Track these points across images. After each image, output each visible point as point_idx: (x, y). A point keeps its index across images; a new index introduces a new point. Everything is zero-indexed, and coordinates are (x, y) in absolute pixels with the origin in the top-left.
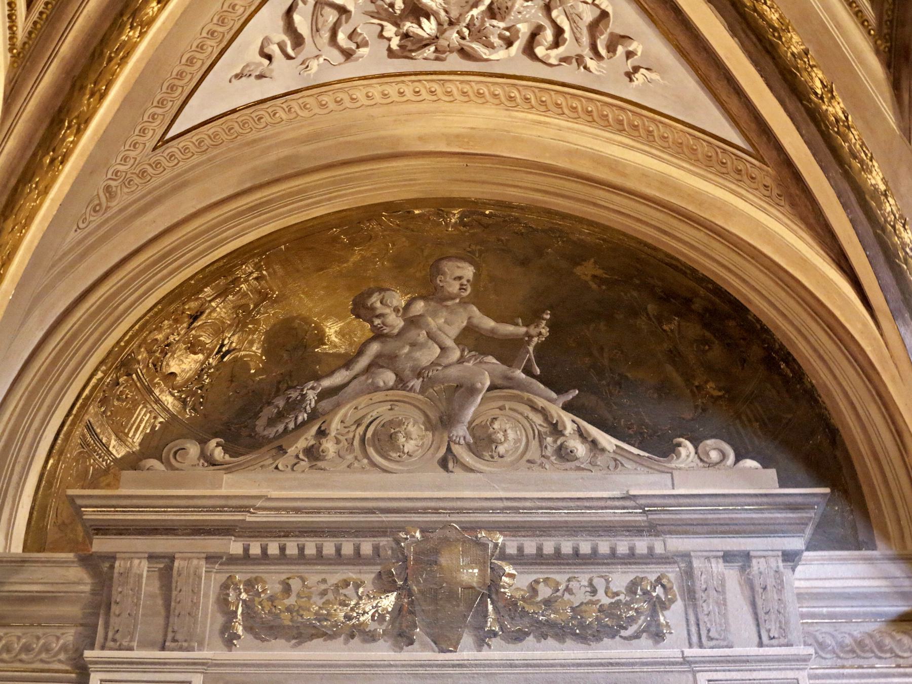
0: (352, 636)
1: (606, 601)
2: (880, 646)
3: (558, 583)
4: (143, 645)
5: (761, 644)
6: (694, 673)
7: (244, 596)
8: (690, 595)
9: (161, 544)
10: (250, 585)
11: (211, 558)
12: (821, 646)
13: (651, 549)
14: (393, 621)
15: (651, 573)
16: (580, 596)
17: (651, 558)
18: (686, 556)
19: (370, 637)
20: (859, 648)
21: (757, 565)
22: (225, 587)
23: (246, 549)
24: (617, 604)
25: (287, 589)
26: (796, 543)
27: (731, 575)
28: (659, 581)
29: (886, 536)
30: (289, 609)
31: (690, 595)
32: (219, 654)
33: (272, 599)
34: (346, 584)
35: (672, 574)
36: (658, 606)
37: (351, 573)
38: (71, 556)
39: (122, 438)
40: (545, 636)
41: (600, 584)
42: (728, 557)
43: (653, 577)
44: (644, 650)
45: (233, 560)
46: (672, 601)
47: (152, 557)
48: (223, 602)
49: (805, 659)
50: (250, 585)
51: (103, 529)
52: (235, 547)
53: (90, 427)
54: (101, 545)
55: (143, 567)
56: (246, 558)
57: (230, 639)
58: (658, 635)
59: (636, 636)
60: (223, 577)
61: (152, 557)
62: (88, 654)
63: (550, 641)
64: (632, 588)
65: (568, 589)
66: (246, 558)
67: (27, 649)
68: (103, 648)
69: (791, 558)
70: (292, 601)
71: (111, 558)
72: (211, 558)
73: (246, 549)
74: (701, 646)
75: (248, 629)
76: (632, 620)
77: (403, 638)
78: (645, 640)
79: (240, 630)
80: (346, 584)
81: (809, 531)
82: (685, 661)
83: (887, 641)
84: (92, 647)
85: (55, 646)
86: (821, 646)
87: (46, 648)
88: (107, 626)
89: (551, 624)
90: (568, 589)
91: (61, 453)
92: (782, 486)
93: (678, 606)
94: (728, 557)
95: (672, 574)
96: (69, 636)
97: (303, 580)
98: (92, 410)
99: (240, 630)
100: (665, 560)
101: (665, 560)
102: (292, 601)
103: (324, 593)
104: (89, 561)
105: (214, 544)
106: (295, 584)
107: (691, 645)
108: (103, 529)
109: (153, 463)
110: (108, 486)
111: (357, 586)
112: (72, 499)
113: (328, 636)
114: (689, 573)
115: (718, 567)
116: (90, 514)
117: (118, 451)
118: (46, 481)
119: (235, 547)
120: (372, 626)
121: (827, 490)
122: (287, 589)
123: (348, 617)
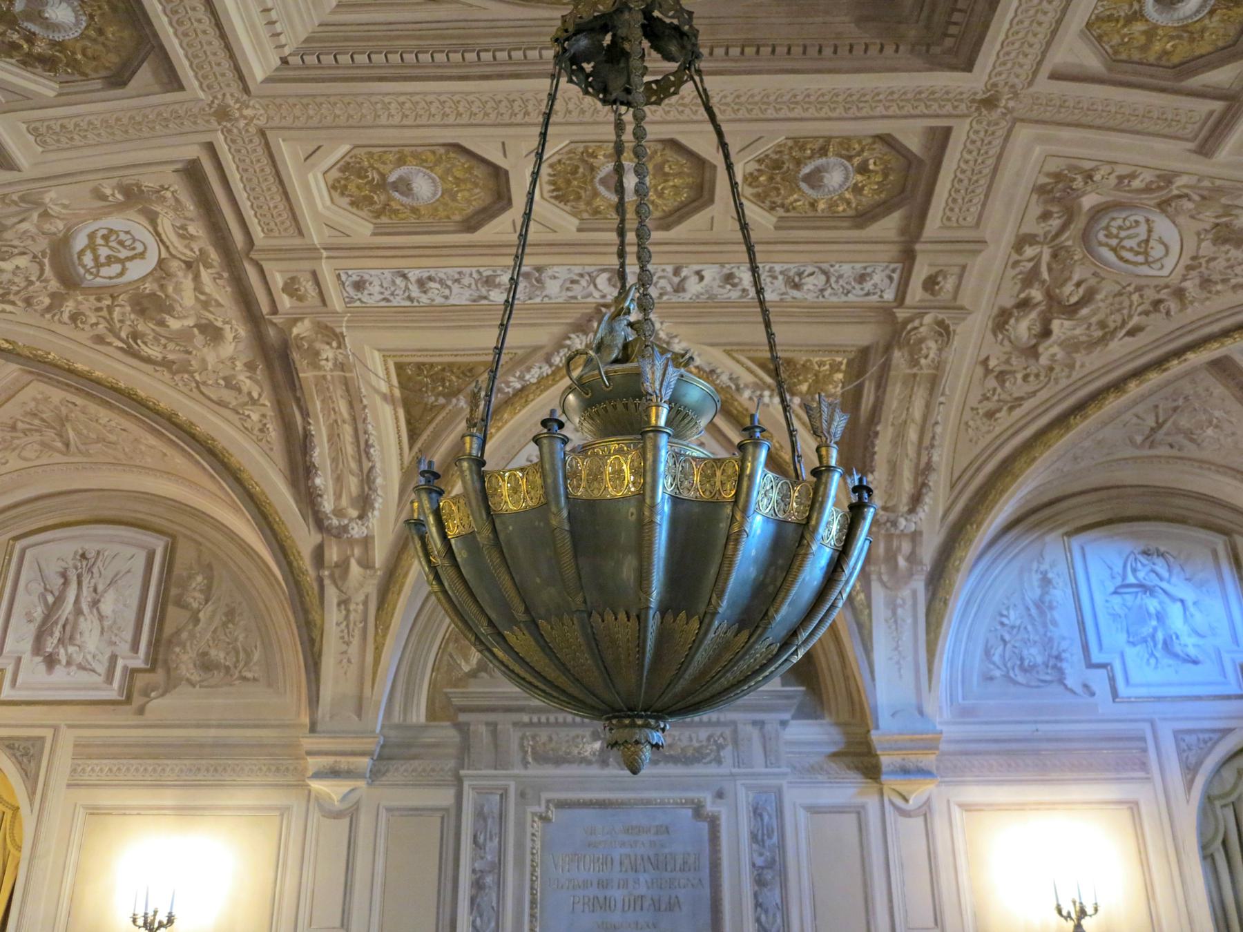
0: (581, 762)
1: (696, 745)
2: (821, 768)
3: (674, 736)
4: (487, 767)
5: (766, 767)
6: (735, 780)
7: (531, 743)
8: (735, 742)
9: (491, 717)
10: (534, 738)
11: (515, 724)
12: (795, 768)
13: (718, 719)
14: (599, 755)
15: (718, 731)
16: (685, 743)
17: (718, 723)
18: (734, 723)
19: (588, 762)
20: (812, 769)
21: (768, 727)
22: (522, 739)
23: (531, 719)
24: (702, 746)
25: (551, 739)
26: (786, 716)
27: (755, 733)
28: (721, 735)
29: (830, 713)
30: (552, 750)
31: (735, 742)
32: (522, 772)
33: (544, 744)
34: (578, 736)
35: (728, 732)
36: (720, 747)
37: (579, 731)
38: (448, 723)
39: (467, 661)
40: (668, 762)
41: (693, 735)
42: (754, 723)
43: (718, 733)
44: (713, 769)
45: (525, 725)
46: (727, 745)
47: (487, 724)
48: (522, 746)
49: (785, 774)
50: (534, 738)
51: (463, 710)
52: (526, 718)
53: (451, 656)
54: (462, 718)
55: (483, 729)
56: (531, 724)
57: (525, 764)
58: (719, 761)
59: (710, 762)
60: (520, 734)
61: (487, 724)
62: (462, 772)
63: (671, 765)
64: (709, 739)
65: (680, 740)
66: (531, 724)
67: (433, 770)
68: (468, 769)
69: (784, 724)
70: (553, 745)
71: (468, 724)
72: (515, 724)
73: (531, 719)
74: (739, 767)
75: (534, 759)
76: (708, 754)
77: (604, 763)
78: (714, 764)
79: (530, 760)
80: (578, 736)
81: (793, 711)
82: (732, 775)
83: (825, 766)
84: (463, 768)
85: (447, 768)
86: (795, 768)
87: (442, 770)
88: (469, 757)
89: (671, 756)
90: (680, 740)
91: (438, 669)
92: (783, 685)
93: (730, 747)
94: (754, 723)
95: (728, 732)
96: (452, 764)
97: (558, 734)
98: (451, 645)
99: (530, 760)
100: (725, 724)
101: (725, 724)
102: (553, 745)
103: (568, 741)
104: (459, 727)
105: (515, 717)
106: (554, 737)
107: (734, 766)
108: (463, 710)
109: (483, 674)
110: (464, 687)
111: (583, 737)
112: (446, 694)
113: (570, 762)
114: (735, 731)
115: (749, 728)
116: (456, 701)
117: (466, 668)
118: (433, 685)
119: (526, 718)
120: (590, 757)
121: (802, 688)
122: (551, 739)
123: (579, 753)
